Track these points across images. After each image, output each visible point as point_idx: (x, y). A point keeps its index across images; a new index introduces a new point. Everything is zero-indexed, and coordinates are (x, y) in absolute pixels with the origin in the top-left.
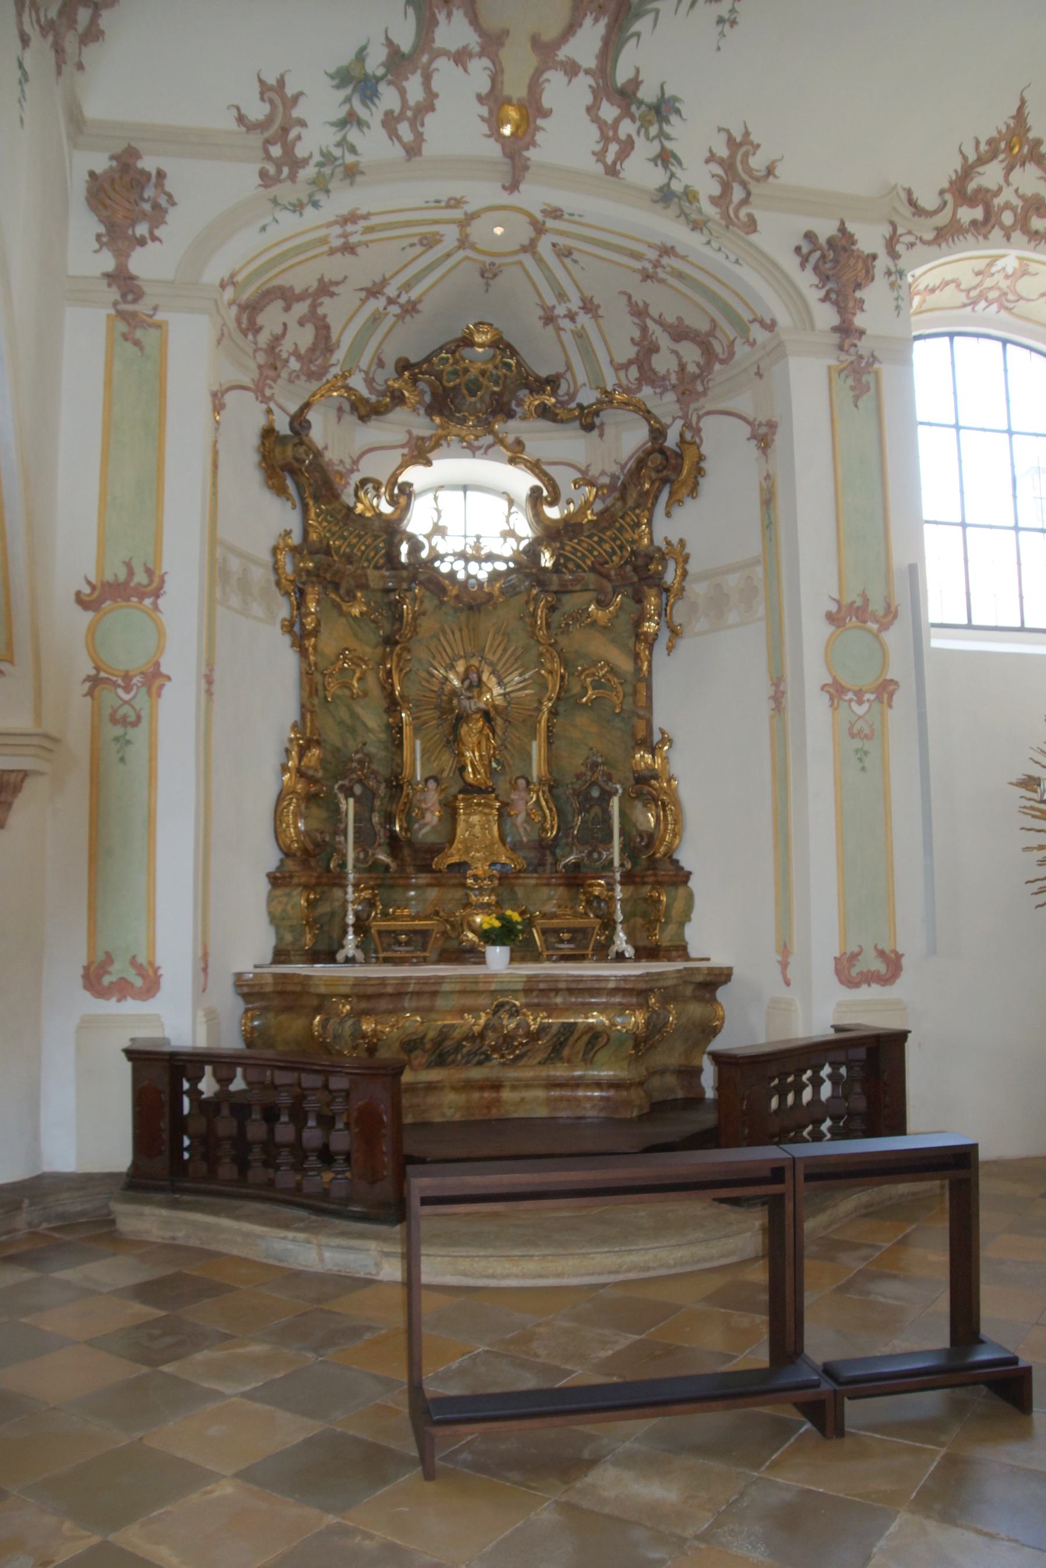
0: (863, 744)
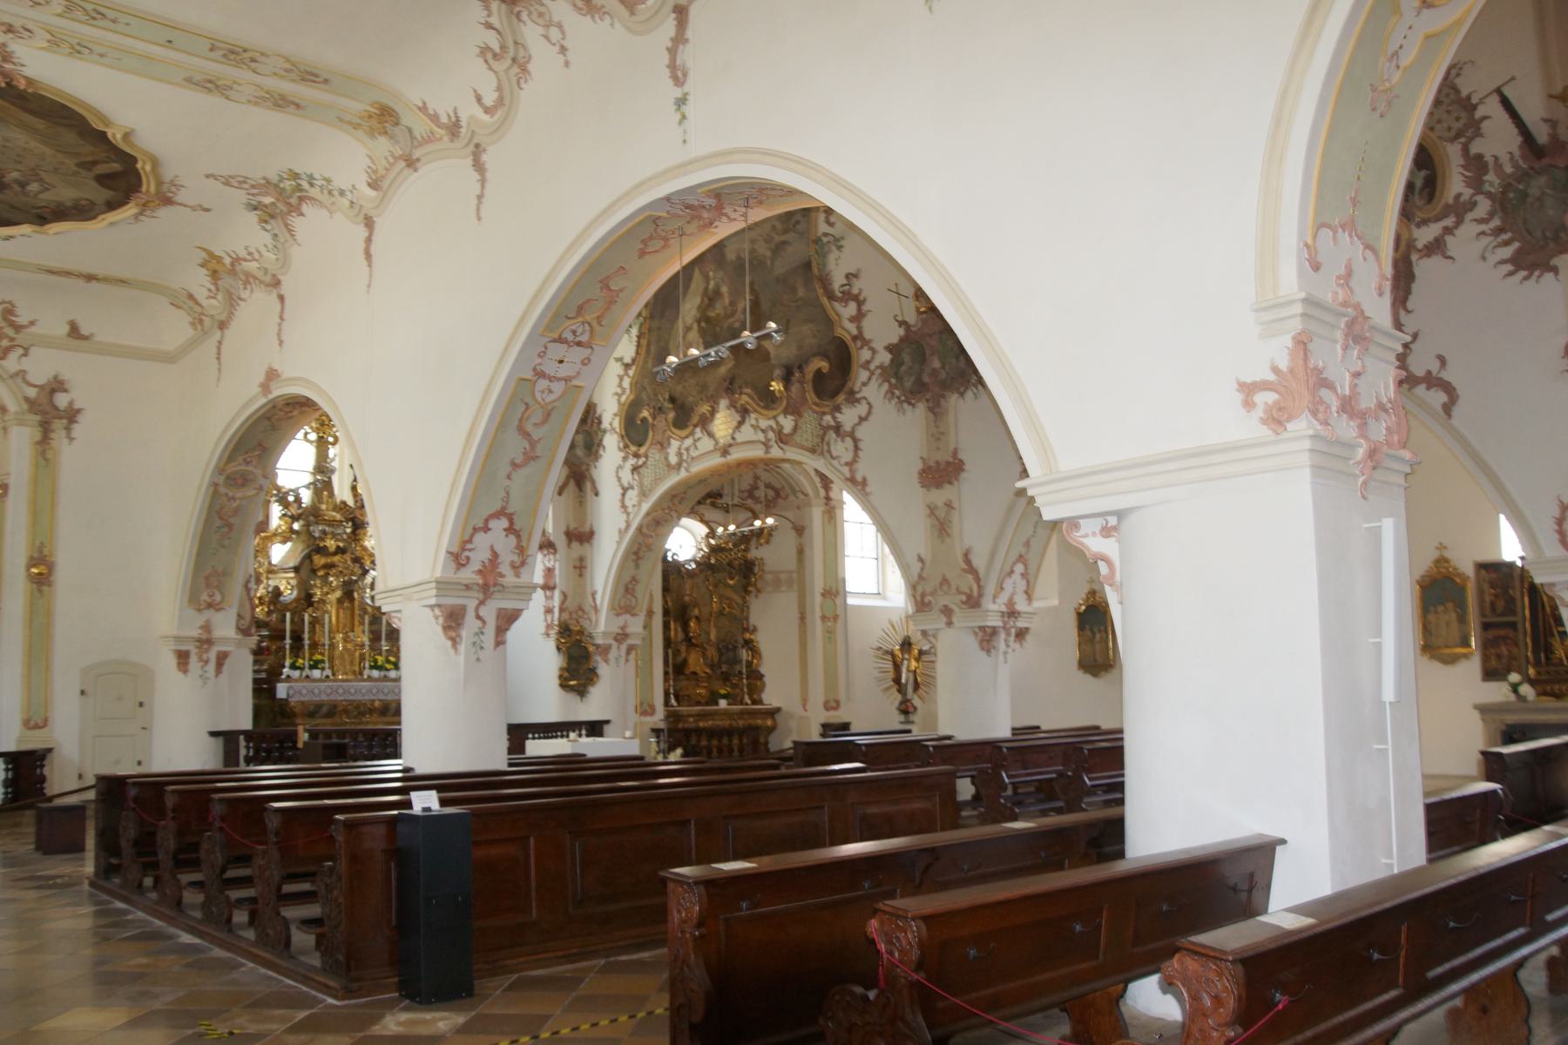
0: (830, 634)
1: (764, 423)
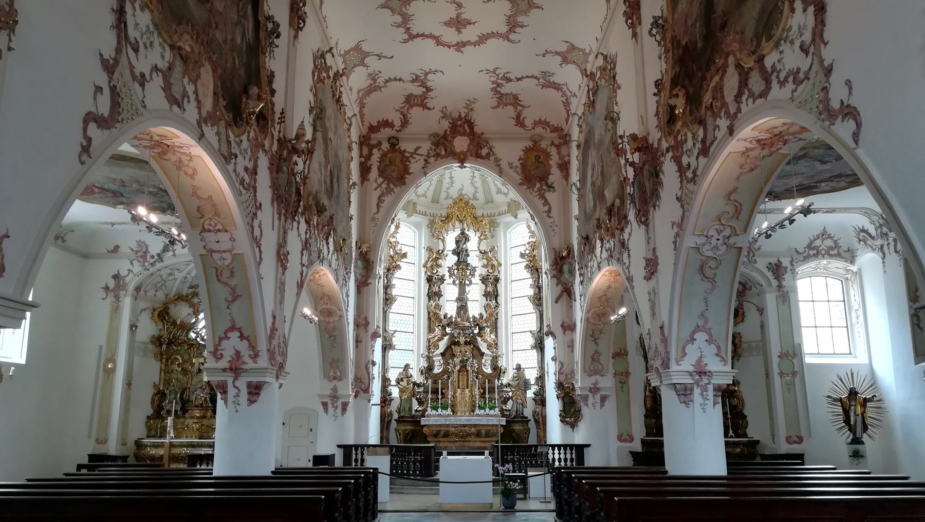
1: (608, 245)
